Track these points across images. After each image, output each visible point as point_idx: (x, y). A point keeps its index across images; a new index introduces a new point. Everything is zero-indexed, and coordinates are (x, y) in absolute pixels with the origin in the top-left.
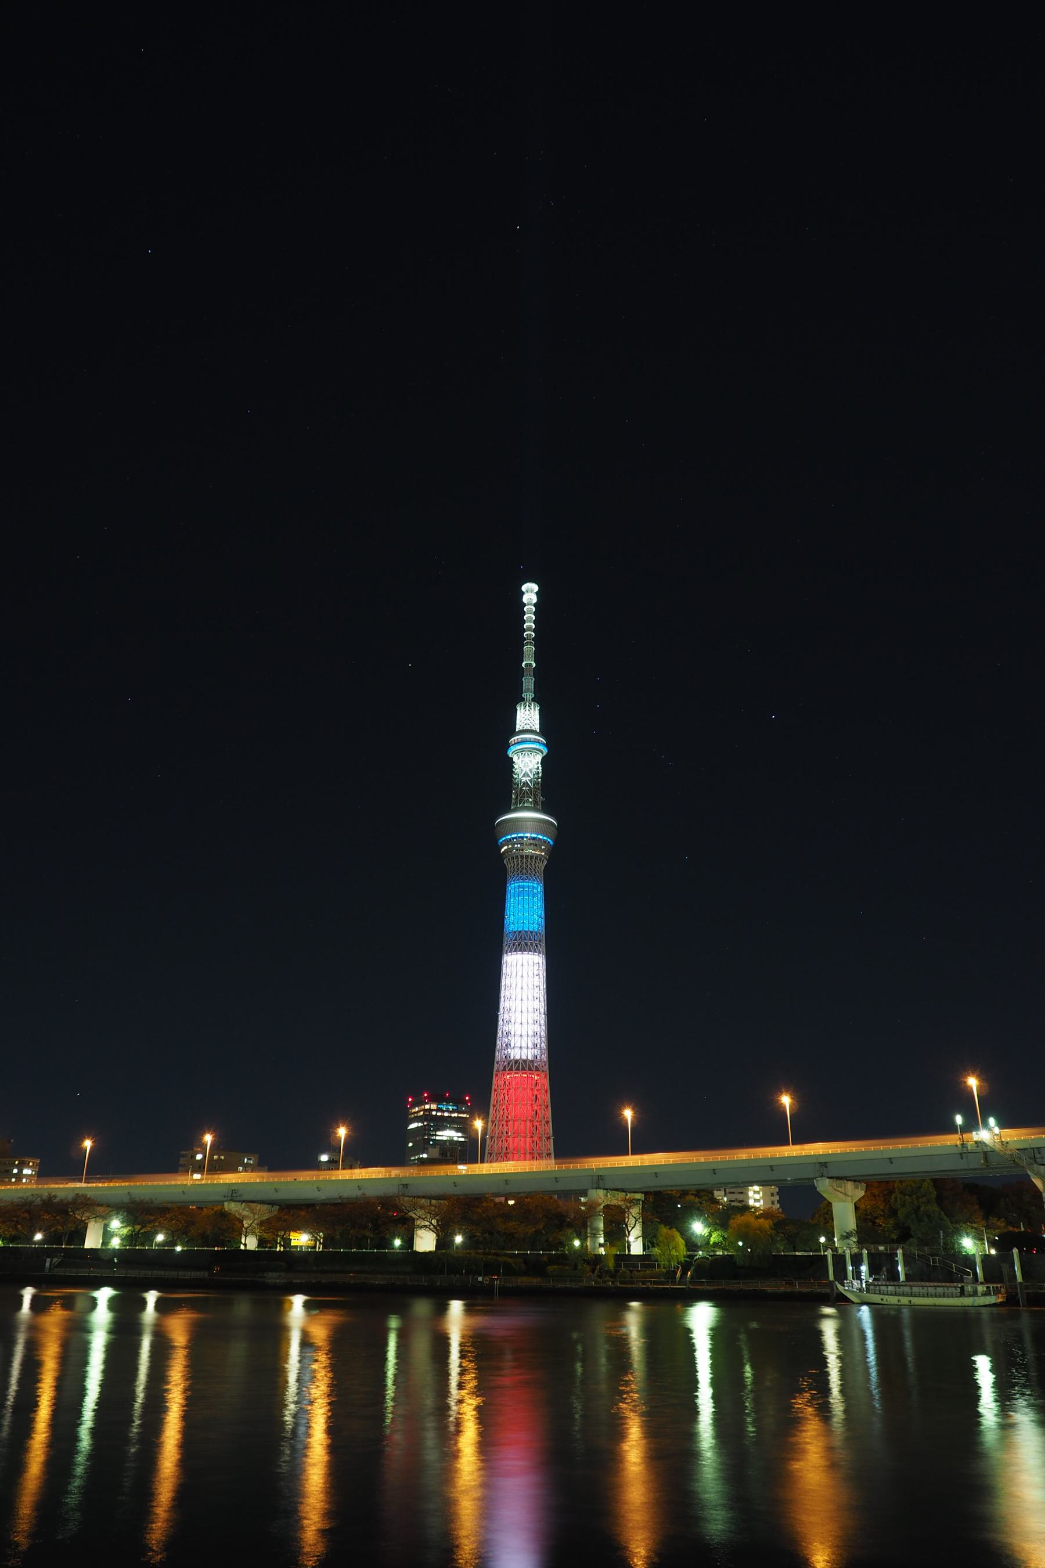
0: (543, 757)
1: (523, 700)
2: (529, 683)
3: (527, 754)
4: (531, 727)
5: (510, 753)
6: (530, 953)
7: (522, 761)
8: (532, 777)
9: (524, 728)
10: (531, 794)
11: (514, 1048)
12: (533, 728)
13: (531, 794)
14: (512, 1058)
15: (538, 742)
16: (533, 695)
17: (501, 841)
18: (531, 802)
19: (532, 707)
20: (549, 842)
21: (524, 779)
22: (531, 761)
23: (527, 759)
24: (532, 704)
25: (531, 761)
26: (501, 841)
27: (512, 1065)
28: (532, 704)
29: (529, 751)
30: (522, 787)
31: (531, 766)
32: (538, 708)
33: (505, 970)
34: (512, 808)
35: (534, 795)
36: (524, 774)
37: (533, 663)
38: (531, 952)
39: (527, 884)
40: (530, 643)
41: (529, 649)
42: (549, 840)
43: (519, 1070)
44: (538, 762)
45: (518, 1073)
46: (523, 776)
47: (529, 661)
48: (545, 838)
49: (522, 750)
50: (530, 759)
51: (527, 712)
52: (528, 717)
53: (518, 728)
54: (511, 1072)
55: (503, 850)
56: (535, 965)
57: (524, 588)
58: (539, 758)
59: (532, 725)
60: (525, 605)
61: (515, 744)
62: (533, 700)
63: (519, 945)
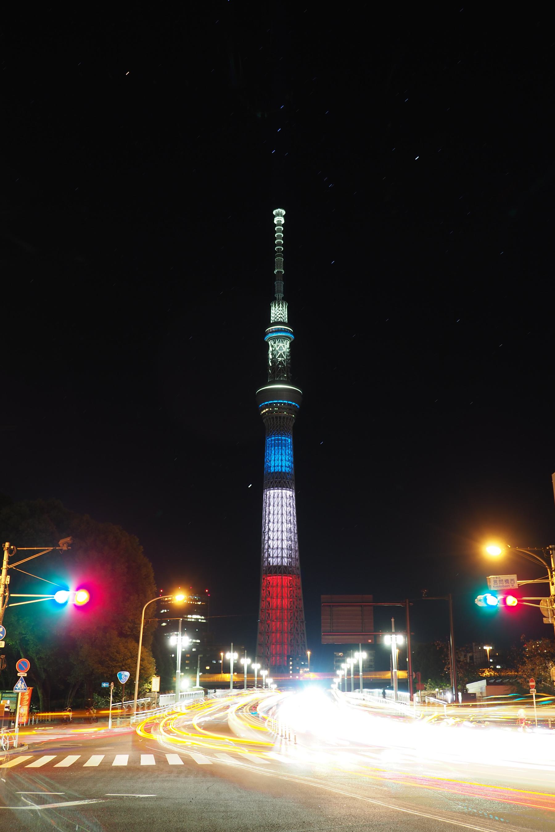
2: (279, 285)
3: (281, 340)
6: (287, 489)
7: (278, 346)
8: (285, 358)
9: (279, 321)
10: (285, 371)
11: (272, 557)
13: (285, 371)
14: (271, 564)
16: (283, 295)
17: (261, 406)
19: (284, 305)
20: (297, 406)
21: (280, 359)
22: (284, 346)
23: (281, 344)
24: (284, 303)
25: (284, 346)
26: (261, 406)
27: (271, 570)
28: (284, 303)
29: (283, 338)
34: (269, 381)
36: (280, 355)
37: (283, 271)
38: (288, 488)
39: (284, 438)
41: (279, 259)
42: (297, 405)
43: (276, 573)
45: (276, 576)
47: (279, 270)
48: (294, 404)
49: (277, 338)
50: (283, 344)
51: (281, 308)
54: (270, 575)
55: (262, 413)
57: (274, 213)
59: (284, 319)
62: (284, 299)
63: (280, 482)
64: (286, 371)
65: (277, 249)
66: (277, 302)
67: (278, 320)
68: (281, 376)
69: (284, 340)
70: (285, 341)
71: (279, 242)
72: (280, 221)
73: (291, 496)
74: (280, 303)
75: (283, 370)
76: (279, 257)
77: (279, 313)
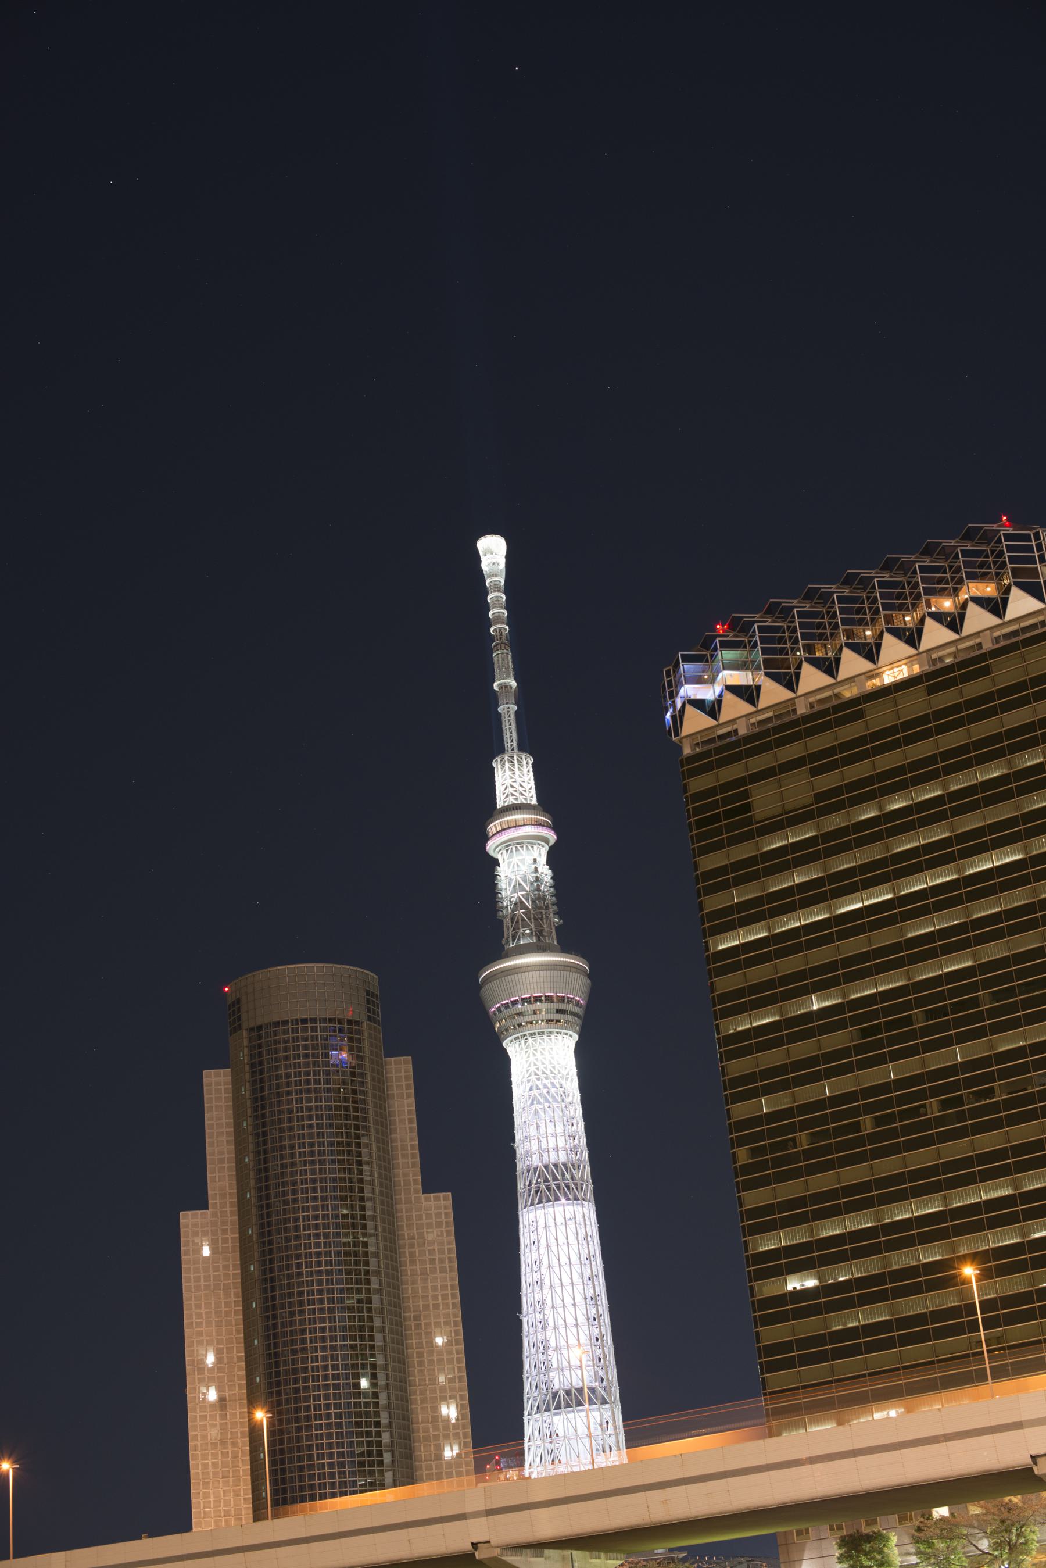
0: (550, 848)
1: (501, 750)
3: (514, 849)
4: (516, 799)
9: (506, 804)
12: (522, 800)
15: (538, 824)
19: (515, 762)
22: (523, 861)
29: (518, 844)
30: (513, 911)
32: (531, 760)
33: (526, 1237)
35: (535, 919)
36: (515, 886)
49: (507, 845)
53: (500, 803)
56: (569, 1222)
58: (541, 853)
61: (498, 832)
64: (533, 920)
65: (493, 631)
66: (499, 760)
67: (505, 802)
68: (521, 935)
69: (522, 847)
70: (524, 847)
71: (496, 615)
72: (494, 564)
73: (568, 1216)
74: (504, 764)
75: (523, 919)
76: (498, 650)
77: (505, 786)
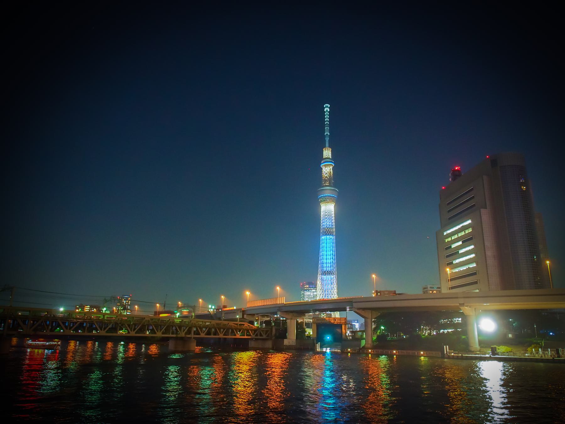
5: (321, 167)
18: (328, 183)
22: (328, 169)
23: (327, 168)
25: (328, 169)
31: (328, 170)
40: (327, 126)
41: (327, 128)
44: (330, 169)
46: (326, 174)
47: (327, 133)
49: (325, 165)
52: (327, 153)
53: (324, 157)
57: (325, 105)
58: (331, 167)
60: (325, 112)
